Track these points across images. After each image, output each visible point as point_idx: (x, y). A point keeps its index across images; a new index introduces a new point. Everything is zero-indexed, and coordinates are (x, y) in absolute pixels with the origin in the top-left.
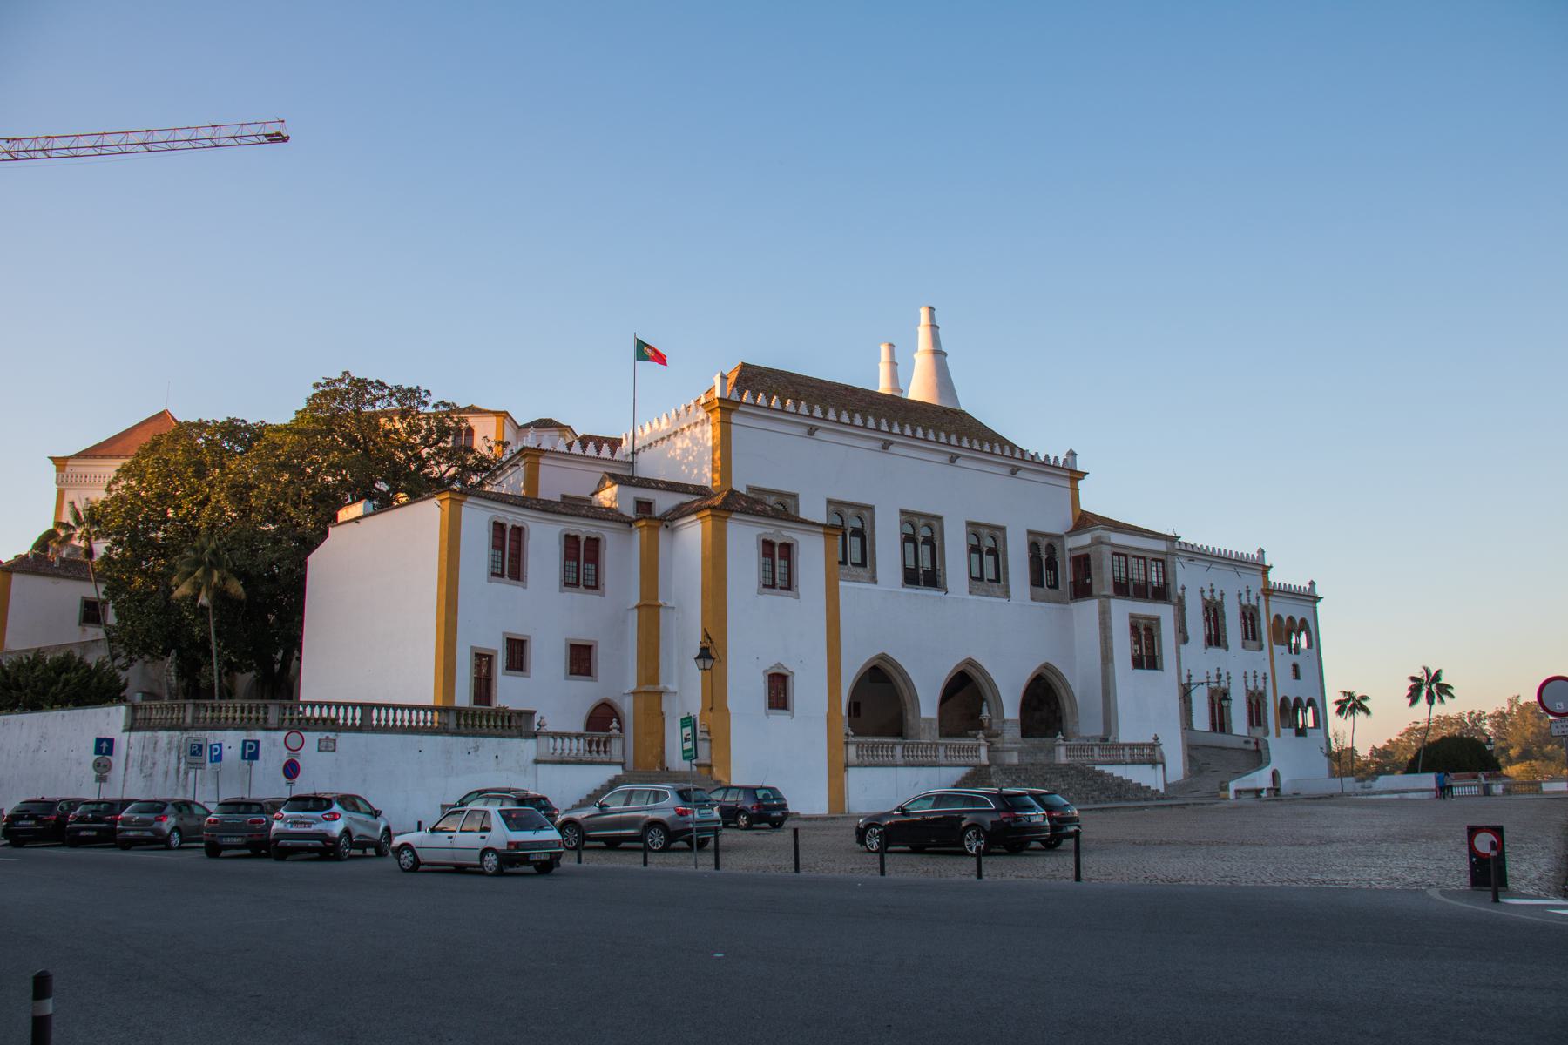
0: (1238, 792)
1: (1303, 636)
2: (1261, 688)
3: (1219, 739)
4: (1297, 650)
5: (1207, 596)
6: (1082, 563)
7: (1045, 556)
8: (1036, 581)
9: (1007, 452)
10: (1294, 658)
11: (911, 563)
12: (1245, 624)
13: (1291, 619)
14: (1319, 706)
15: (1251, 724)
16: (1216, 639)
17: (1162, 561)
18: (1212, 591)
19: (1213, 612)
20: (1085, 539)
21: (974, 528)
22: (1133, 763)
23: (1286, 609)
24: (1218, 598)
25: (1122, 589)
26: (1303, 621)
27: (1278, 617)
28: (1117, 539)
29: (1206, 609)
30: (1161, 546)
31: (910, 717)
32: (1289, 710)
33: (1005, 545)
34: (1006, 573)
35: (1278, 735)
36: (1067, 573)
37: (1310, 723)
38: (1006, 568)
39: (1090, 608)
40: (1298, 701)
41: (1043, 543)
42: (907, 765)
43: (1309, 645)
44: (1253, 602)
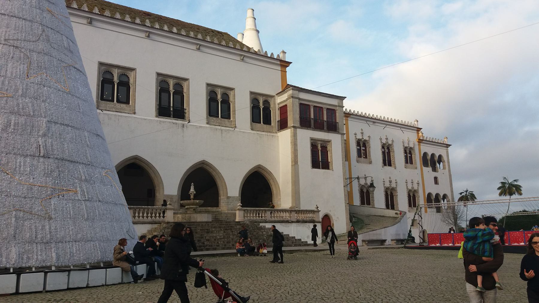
0: (363, 241)
1: (441, 164)
2: (416, 188)
3: (391, 213)
5: (384, 141)
6: (283, 110)
9: (238, 47)
10: (435, 174)
13: (433, 155)
14: (450, 198)
15: (410, 205)
16: (387, 161)
17: (332, 112)
18: (387, 139)
20: (285, 97)
22: (298, 221)
23: (430, 150)
24: (390, 143)
25: (305, 123)
26: (440, 156)
27: (425, 154)
28: (303, 96)
29: (383, 147)
30: (335, 102)
32: (434, 200)
35: (426, 212)
40: (437, 195)
43: (444, 168)
44: (411, 146)
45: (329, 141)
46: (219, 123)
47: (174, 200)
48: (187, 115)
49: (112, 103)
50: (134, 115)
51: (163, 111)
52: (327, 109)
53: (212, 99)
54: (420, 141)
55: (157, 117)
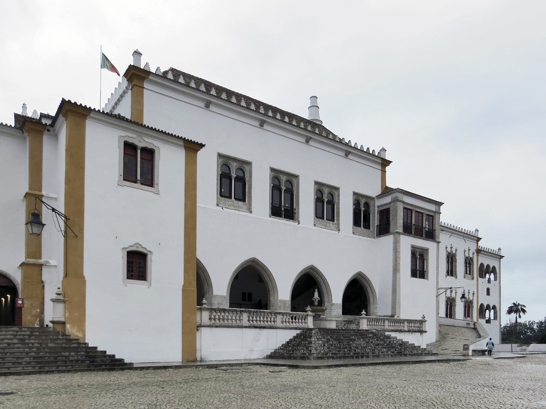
1: (492, 275)
4: (489, 281)
6: (385, 214)
7: (363, 209)
8: (356, 223)
10: (489, 285)
11: (277, 204)
12: (466, 266)
13: (488, 266)
18: (451, 248)
19: (451, 259)
21: (320, 187)
24: (454, 252)
25: (407, 230)
26: (494, 268)
27: (482, 265)
29: (448, 257)
31: (272, 299)
33: (339, 199)
34: (338, 216)
36: (375, 220)
37: (492, 317)
38: (338, 213)
39: (388, 239)
41: (363, 201)
42: (249, 327)
43: (495, 279)
44: (471, 256)
45: (427, 250)
46: (326, 226)
47: (287, 305)
48: (296, 216)
49: (231, 200)
50: (249, 214)
51: (276, 211)
52: (427, 215)
53: (319, 200)
54: (479, 251)
55: (270, 217)
